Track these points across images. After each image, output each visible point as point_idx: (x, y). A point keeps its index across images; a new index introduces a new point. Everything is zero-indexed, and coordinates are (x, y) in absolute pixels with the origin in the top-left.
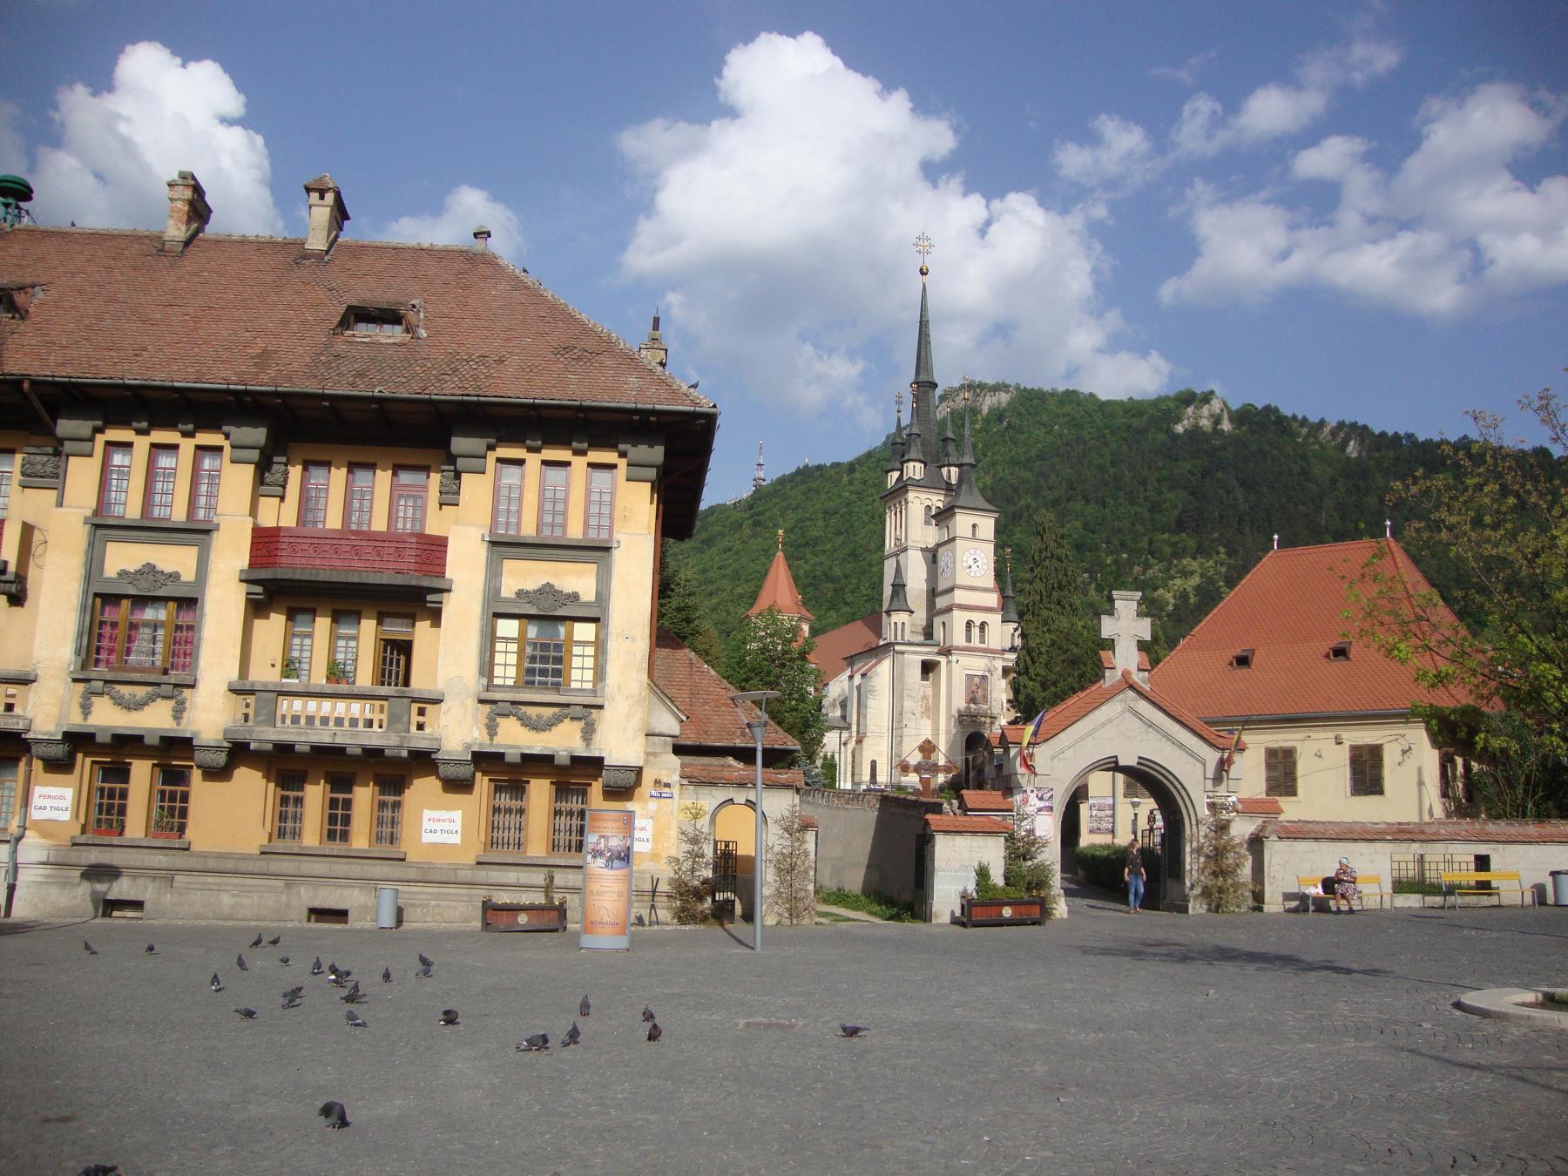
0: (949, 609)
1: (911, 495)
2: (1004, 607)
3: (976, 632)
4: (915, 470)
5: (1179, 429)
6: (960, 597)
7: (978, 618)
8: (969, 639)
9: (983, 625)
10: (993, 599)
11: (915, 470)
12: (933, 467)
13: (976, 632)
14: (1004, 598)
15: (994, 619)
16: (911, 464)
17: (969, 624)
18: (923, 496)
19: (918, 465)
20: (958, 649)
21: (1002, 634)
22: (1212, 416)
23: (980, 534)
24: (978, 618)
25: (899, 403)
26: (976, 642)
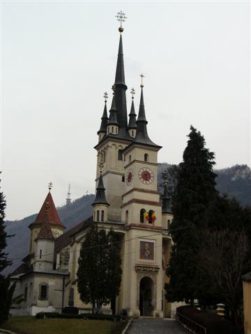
0: (131, 202)
2: (164, 202)
5: (234, 179)
6: (137, 195)
7: (148, 208)
8: (142, 220)
9: (151, 212)
10: (156, 198)
12: (123, 130)
15: (158, 211)
16: (111, 127)
17: (142, 211)
18: (117, 144)
19: (115, 127)
20: (135, 225)
21: (162, 219)
22: (246, 174)
24: (148, 208)
25: (106, 97)
26: (147, 223)
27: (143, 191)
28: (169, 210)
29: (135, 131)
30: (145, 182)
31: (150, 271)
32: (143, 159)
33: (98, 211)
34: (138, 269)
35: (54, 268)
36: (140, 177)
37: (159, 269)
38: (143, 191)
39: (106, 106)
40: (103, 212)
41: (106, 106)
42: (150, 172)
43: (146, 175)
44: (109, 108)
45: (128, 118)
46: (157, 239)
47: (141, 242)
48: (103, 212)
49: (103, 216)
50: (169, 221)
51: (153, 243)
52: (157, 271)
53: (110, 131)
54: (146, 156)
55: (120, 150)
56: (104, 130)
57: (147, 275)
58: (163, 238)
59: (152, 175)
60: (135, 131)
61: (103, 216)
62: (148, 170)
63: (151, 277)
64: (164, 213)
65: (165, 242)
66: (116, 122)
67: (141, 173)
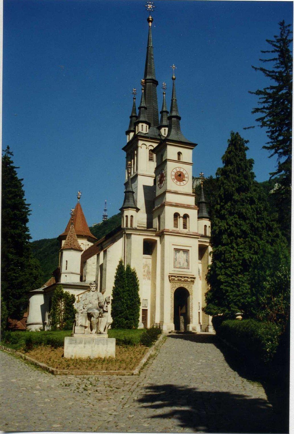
1: (140, 143)
3: (181, 221)
4: (143, 128)
8: (176, 225)
9: (186, 216)
10: (191, 201)
11: (143, 128)
13: (181, 221)
14: (198, 203)
15: (193, 214)
16: (140, 125)
17: (176, 215)
18: (148, 144)
19: (145, 125)
21: (199, 225)
23: (183, 158)
24: (182, 212)
27: (176, 193)
28: (205, 214)
29: (167, 129)
30: (178, 183)
31: (185, 281)
32: (177, 159)
33: (127, 216)
34: (172, 278)
35: (81, 280)
36: (174, 177)
37: (194, 278)
38: (176, 193)
39: (134, 104)
40: (132, 216)
41: (134, 104)
42: (184, 172)
43: (180, 175)
44: (137, 106)
45: (160, 115)
46: (194, 245)
47: (174, 249)
48: (132, 216)
49: (132, 221)
50: (206, 226)
51: (189, 250)
52: (193, 282)
53: (140, 130)
54: (179, 154)
55: (151, 150)
56: (132, 129)
57: (182, 285)
58: (200, 245)
59: (186, 176)
60: (167, 129)
61: (132, 221)
62: (182, 170)
63: (186, 287)
64: (200, 218)
65: (202, 250)
66: (147, 120)
67: (173, 174)
